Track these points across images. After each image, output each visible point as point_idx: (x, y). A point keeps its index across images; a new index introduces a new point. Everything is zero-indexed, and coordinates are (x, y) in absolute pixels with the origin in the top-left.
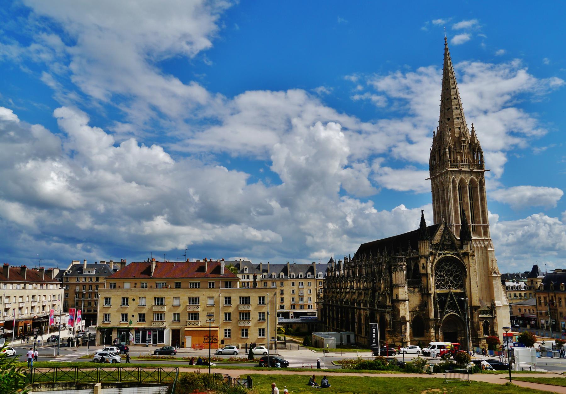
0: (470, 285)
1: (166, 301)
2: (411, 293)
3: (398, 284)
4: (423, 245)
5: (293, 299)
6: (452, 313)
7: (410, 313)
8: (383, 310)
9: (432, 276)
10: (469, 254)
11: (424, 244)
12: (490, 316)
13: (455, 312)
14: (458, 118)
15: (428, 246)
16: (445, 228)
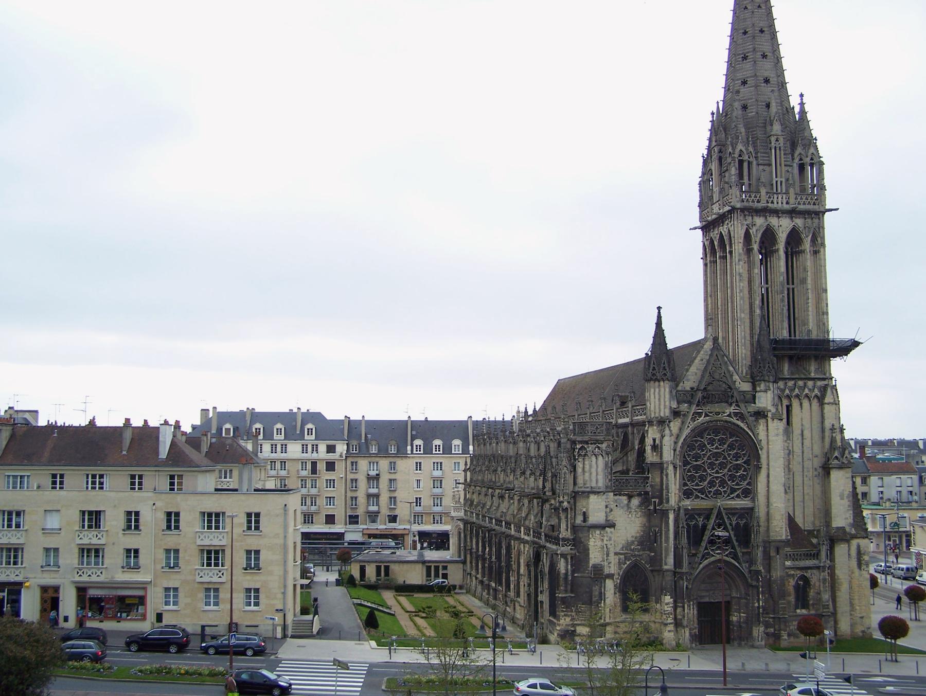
0: (768, 491)
1: (28, 521)
2: (622, 508)
3: (588, 487)
4: (657, 393)
5: (418, 501)
6: (718, 557)
7: (617, 557)
8: (554, 547)
9: (675, 467)
10: (770, 415)
11: (657, 390)
13: (727, 556)
15: (667, 396)
16: (712, 350)
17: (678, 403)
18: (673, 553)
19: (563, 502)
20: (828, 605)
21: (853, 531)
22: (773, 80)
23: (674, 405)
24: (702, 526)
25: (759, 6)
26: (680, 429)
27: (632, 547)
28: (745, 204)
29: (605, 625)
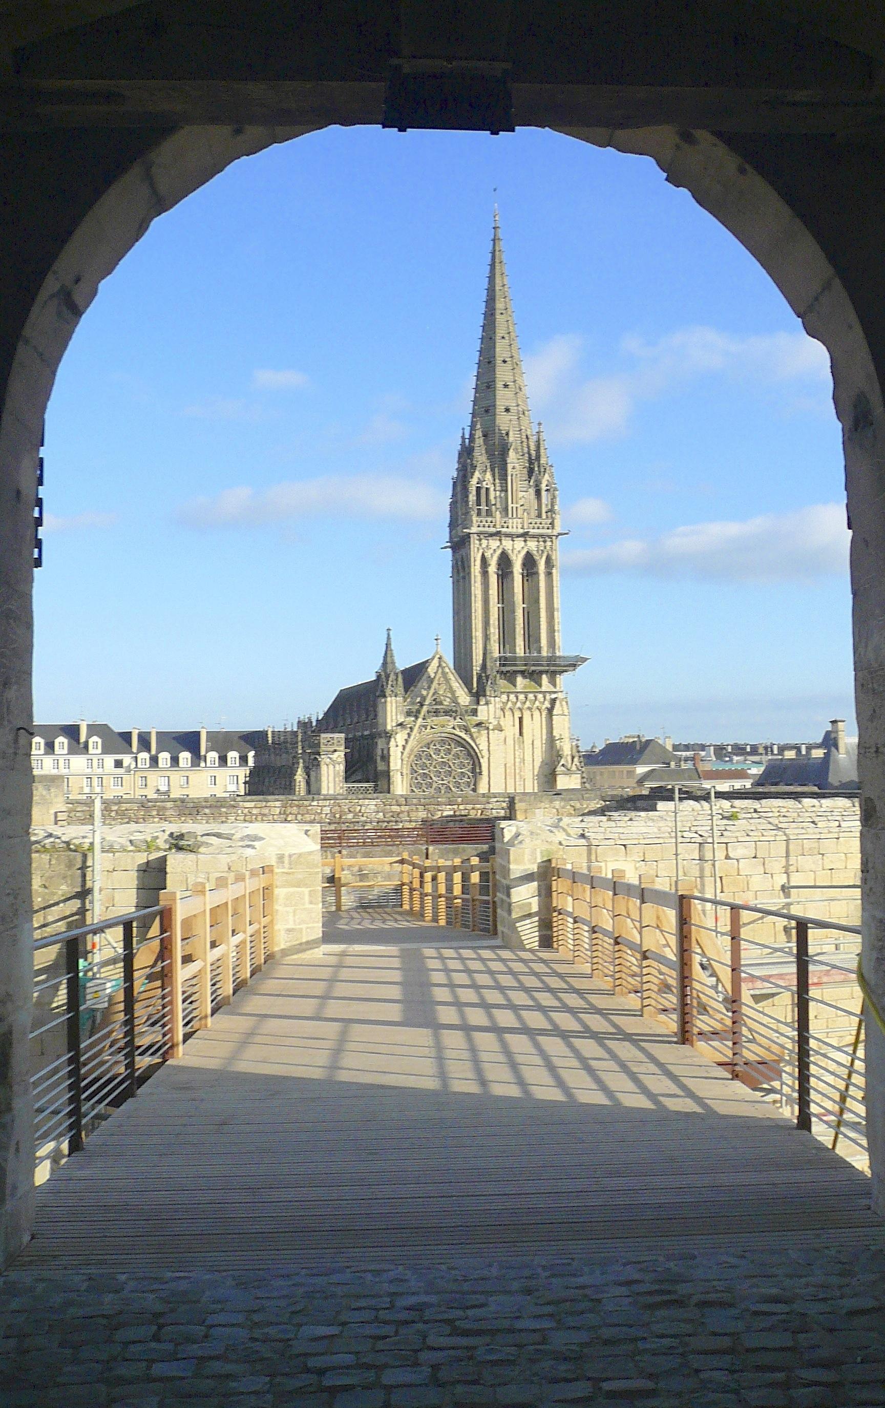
10: (491, 727)
17: (405, 718)
22: (513, 409)
23: (401, 719)
28: (481, 529)
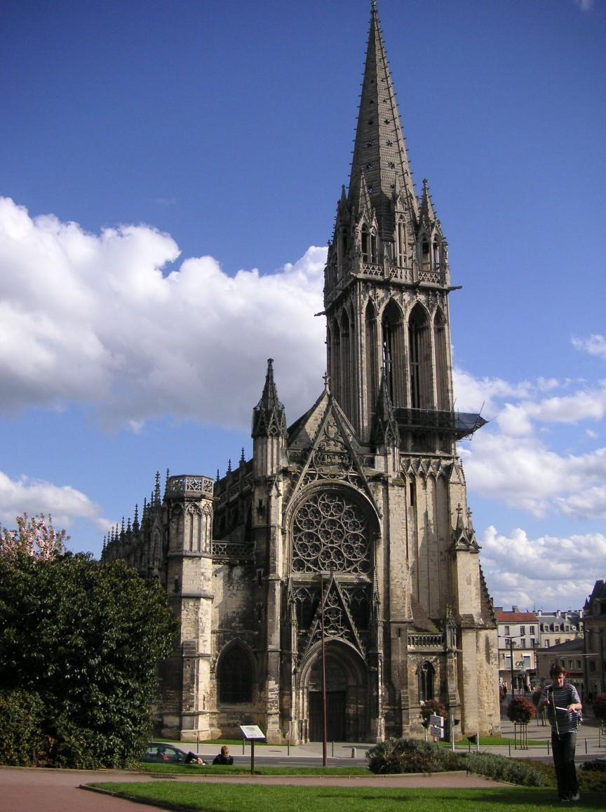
6: (332, 638)
9: (283, 533)
10: (390, 481)
12: (439, 648)
13: (342, 636)
14: (392, 165)
18: (279, 631)
19: (153, 569)
20: (454, 696)
21: (481, 621)
24: (314, 601)
25: (384, 101)
26: (290, 492)
27: (233, 624)
28: (368, 276)
29: (197, 714)
